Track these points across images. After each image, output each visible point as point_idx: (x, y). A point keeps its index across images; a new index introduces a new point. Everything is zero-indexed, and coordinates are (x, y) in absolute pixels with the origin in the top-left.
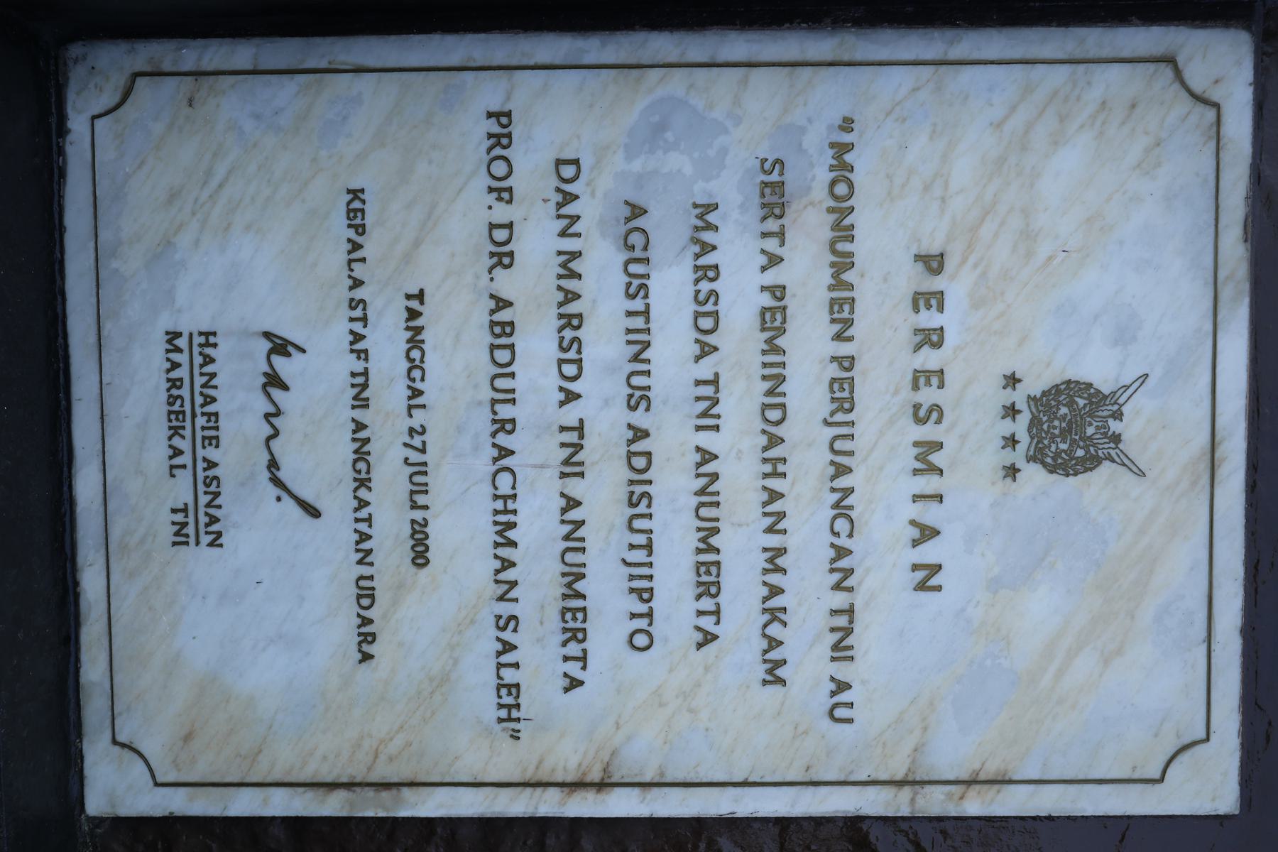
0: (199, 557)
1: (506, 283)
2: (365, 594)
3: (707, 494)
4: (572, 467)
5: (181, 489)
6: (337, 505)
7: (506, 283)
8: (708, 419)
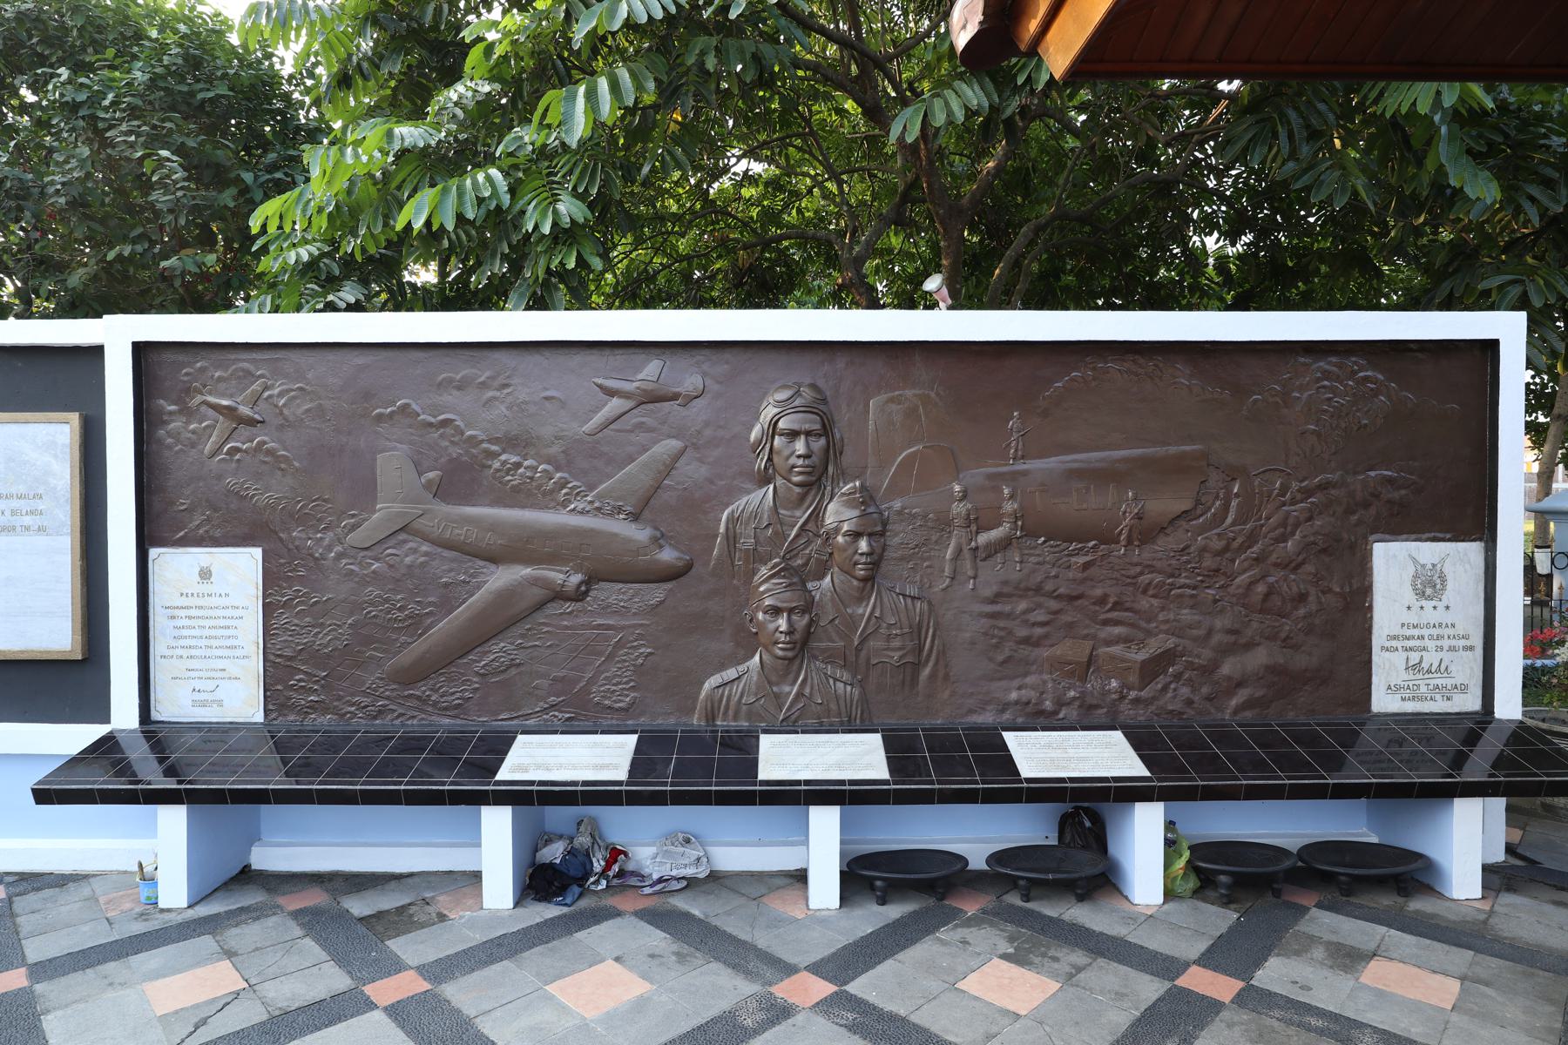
0: (224, 703)
1: (185, 656)
2: (230, 678)
3: (215, 628)
4: (211, 647)
5: (215, 706)
6: (217, 682)
7: (185, 656)
8: (204, 627)
